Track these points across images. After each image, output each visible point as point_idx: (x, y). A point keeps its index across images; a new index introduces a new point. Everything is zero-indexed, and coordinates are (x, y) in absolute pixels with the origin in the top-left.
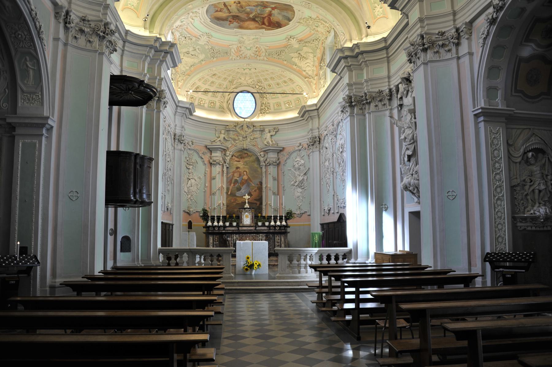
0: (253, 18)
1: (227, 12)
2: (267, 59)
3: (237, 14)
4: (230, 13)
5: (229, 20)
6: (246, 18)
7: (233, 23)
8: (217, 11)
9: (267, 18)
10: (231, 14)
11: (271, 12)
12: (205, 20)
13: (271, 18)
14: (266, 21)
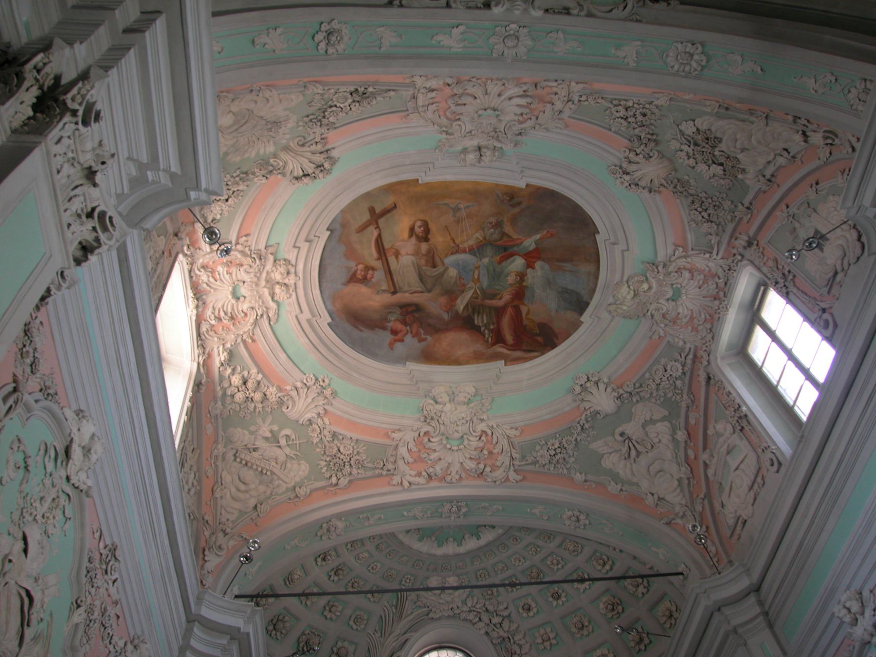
0: (465, 314)
1: (384, 286)
2: (519, 477)
3: (416, 298)
4: (394, 293)
5: (390, 325)
6: (446, 317)
7: (402, 341)
8: (353, 279)
9: (510, 310)
10: (399, 297)
11: (522, 276)
12: (313, 316)
13: (524, 310)
14: (506, 322)
